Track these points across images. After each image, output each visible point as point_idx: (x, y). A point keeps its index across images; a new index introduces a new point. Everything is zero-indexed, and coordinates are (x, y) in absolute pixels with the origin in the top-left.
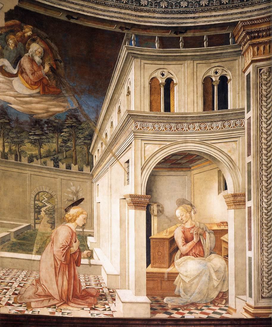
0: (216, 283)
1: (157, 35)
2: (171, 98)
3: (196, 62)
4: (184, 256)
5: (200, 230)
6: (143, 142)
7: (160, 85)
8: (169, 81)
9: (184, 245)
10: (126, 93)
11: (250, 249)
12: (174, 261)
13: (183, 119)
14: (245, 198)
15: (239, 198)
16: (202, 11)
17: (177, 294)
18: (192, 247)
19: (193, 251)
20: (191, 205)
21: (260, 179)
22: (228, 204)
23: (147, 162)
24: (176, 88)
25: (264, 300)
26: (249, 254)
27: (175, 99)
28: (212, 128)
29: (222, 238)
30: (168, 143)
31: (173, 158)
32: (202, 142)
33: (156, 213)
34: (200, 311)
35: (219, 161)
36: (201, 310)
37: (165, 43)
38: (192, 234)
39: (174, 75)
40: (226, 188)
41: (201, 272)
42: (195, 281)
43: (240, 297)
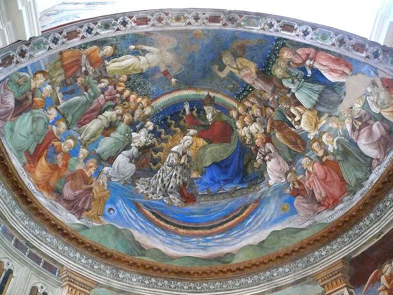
1: (16, 237)
2: (7, 284)
7: (4, 269)
16: (46, 244)
24: (13, 280)
27: (9, 286)
37: (17, 244)
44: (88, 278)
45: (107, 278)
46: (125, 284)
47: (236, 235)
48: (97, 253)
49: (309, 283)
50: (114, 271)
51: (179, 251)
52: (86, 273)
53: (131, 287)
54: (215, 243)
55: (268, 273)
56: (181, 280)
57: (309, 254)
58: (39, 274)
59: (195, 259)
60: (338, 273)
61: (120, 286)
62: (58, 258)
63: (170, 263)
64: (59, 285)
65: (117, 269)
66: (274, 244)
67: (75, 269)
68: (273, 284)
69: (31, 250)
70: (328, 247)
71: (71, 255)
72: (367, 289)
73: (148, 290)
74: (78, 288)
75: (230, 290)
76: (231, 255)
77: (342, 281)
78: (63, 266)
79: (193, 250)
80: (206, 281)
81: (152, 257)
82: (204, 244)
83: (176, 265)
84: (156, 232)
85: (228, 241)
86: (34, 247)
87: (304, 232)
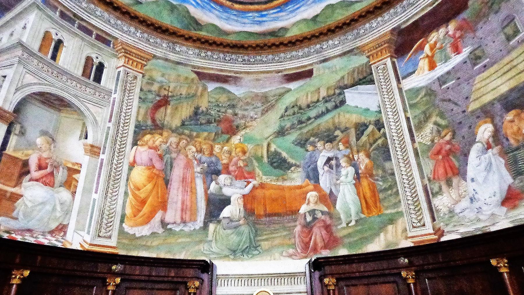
0: (58, 214)
1: (60, 8)
3: (83, 43)
4: (33, 180)
5: (56, 164)
6: (25, 70)
7: (52, 39)
8: (59, 43)
9: (36, 171)
10: (22, 26)
11: (96, 192)
12: (21, 183)
13: (63, 72)
14: (100, 151)
15: (95, 150)
16: (96, 17)
17: (16, 217)
18: (43, 175)
19: (44, 179)
20: (53, 140)
21: (115, 142)
22: (86, 151)
23: (23, 87)
24: (64, 49)
25: (99, 239)
26: (94, 196)
28: (86, 91)
29: (74, 176)
30: (48, 83)
31: (48, 96)
32: (76, 96)
33: (17, 132)
34: (35, 239)
35: (85, 116)
36: (36, 237)
37: (63, 15)
38: (47, 164)
39: (65, 40)
40: (86, 138)
41: (47, 201)
42: (38, 208)
43: (78, 232)
44: (145, 51)
45: (164, 51)
47: (291, 9)
48: (152, 27)
49: (356, 55)
50: (171, 44)
52: (142, 46)
54: (270, 17)
55: (318, 46)
57: (360, 26)
58: (93, 45)
59: (251, 34)
60: (385, 44)
62: (111, 31)
64: (116, 56)
65: (174, 43)
66: (327, 18)
67: (130, 42)
68: (322, 56)
69: (81, 22)
70: (379, 19)
71: (125, 29)
72: (410, 57)
74: (135, 59)
76: (285, 29)
77: (387, 52)
78: (116, 39)
79: (249, 25)
81: (208, 32)
82: (260, 19)
83: (231, 39)
84: (212, 7)
85: (282, 16)
86: (82, 20)
87: (359, 4)
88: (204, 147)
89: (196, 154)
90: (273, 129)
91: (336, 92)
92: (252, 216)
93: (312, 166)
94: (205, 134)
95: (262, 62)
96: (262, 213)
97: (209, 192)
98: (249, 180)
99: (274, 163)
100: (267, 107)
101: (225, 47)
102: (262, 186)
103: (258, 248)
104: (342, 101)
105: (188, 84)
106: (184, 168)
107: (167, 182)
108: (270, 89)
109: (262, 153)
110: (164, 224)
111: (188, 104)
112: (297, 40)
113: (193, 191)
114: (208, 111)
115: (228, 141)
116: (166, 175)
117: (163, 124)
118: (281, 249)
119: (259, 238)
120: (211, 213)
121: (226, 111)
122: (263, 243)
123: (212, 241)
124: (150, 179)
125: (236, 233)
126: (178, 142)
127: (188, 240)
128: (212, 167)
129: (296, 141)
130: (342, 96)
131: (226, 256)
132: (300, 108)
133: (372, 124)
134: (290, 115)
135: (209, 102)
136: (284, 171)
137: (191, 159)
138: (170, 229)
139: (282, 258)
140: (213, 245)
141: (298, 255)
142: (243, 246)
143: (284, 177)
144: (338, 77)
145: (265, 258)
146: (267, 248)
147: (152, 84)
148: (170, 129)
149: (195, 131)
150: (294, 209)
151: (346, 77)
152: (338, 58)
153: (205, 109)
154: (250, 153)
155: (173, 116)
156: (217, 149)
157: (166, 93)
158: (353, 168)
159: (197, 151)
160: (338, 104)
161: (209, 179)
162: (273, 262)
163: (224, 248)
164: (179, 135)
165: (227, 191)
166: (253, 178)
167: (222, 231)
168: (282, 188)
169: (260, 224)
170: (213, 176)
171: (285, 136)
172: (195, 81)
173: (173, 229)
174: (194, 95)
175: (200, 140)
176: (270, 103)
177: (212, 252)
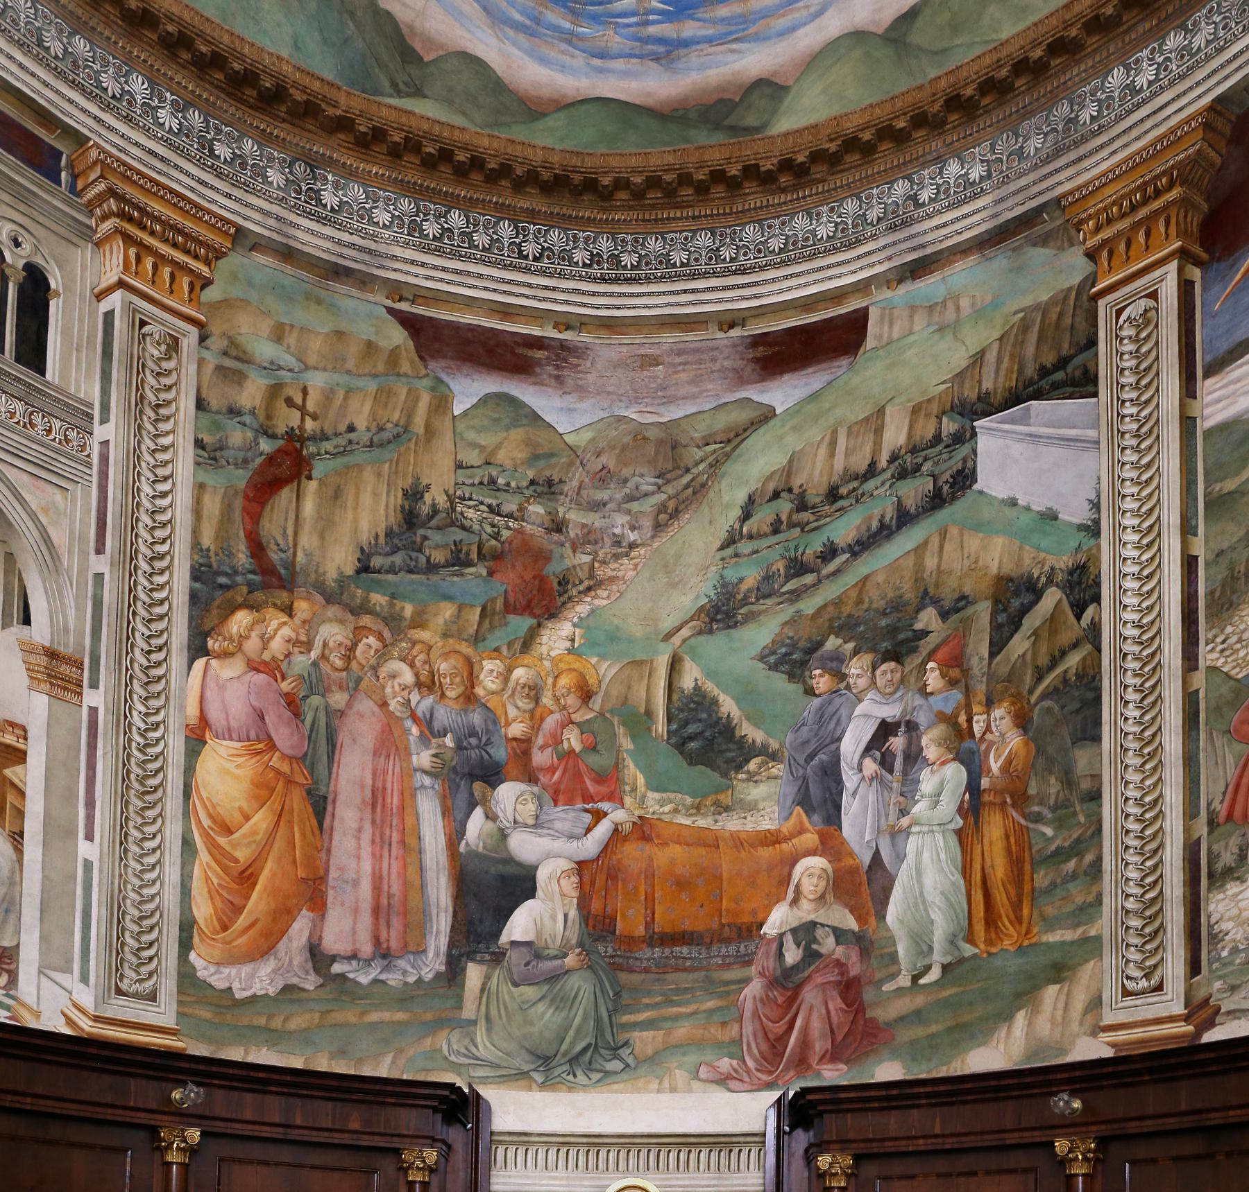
46: (346, 237)
50: (300, 169)
51: (563, 68)
53: (370, 252)
56: (564, 222)
61: (328, 245)
63: (519, 133)
65: (314, 164)
73: (435, 268)
75: (744, 271)
80: (659, 228)
88: (444, 667)
89: (415, 697)
90: (691, 596)
91: (944, 434)
92: (602, 939)
93: (822, 757)
94: (447, 611)
95: (667, 271)
96: (640, 931)
97: (462, 848)
98: (600, 805)
99: (691, 738)
100: (676, 496)
101: (519, 185)
102: (643, 830)
103: (621, 1052)
104: (960, 472)
105: (375, 376)
106: (376, 753)
107: (320, 805)
108: (691, 409)
109: (648, 701)
110: (318, 957)
111: (379, 475)
112: (817, 156)
113: (411, 846)
114: (454, 510)
115: (528, 642)
116: (316, 782)
117: (291, 565)
118: (692, 1059)
119: (626, 1018)
120: (471, 923)
121: (521, 509)
122: (636, 1034)
123: (474, 1023)
124: (262, 790)
125: (553, 1001)
126: (349, 643)
127: (400, 1016)
128: (473, 748)
129: (773, 653)
130: (964, 450)
131: (522, 1075)
132: (802, 505)
133: (1057, 586)
134: (760, 536)
135: (459, 466)
136: (725, 775)
137: (398, 714)
138: (342, 977)
139: (696, 1085)
140: (480, 1034)
141: (746, 1079)
142: (572, 1044)
143: (721, 797)
144: (959, 358)
145: (640, 1083)
146: (650, 1051)
147: (238, 378)
148: (320, 587)
149: (411, 600)
150: (746, 919)
151: (991, 357)
152: (972, 259)
153: (442, 501)
154: (606, 694)
155: (325, 526)
156: (489, 673)
157: (294, 419)
158: (963, 769)
159: (419, 685)
160: (946, 488)
161: (462, 796)
162: (665, 1097)
163: (512, 1046)
164: (352, 612)
165: (524, 846)
166: (615, 797)
167: (506, 989)
168: (711, 841)
169: (631, 970)
170: (478, 786)
171: (735, 626)
172: (405, 367)
173: (351, 976)
174: (403, 432)
175: (425, 635)
176: (688, 478)
177: (477, 1059)
